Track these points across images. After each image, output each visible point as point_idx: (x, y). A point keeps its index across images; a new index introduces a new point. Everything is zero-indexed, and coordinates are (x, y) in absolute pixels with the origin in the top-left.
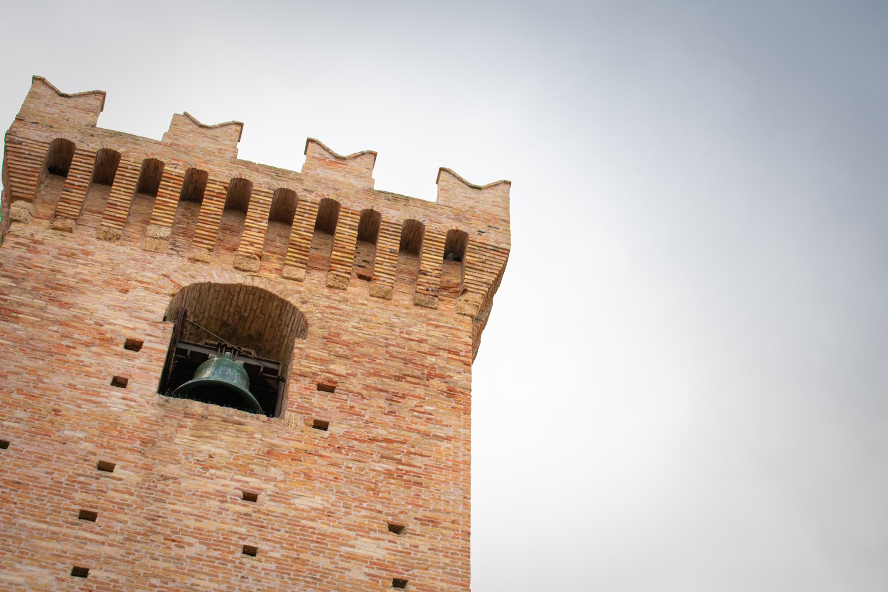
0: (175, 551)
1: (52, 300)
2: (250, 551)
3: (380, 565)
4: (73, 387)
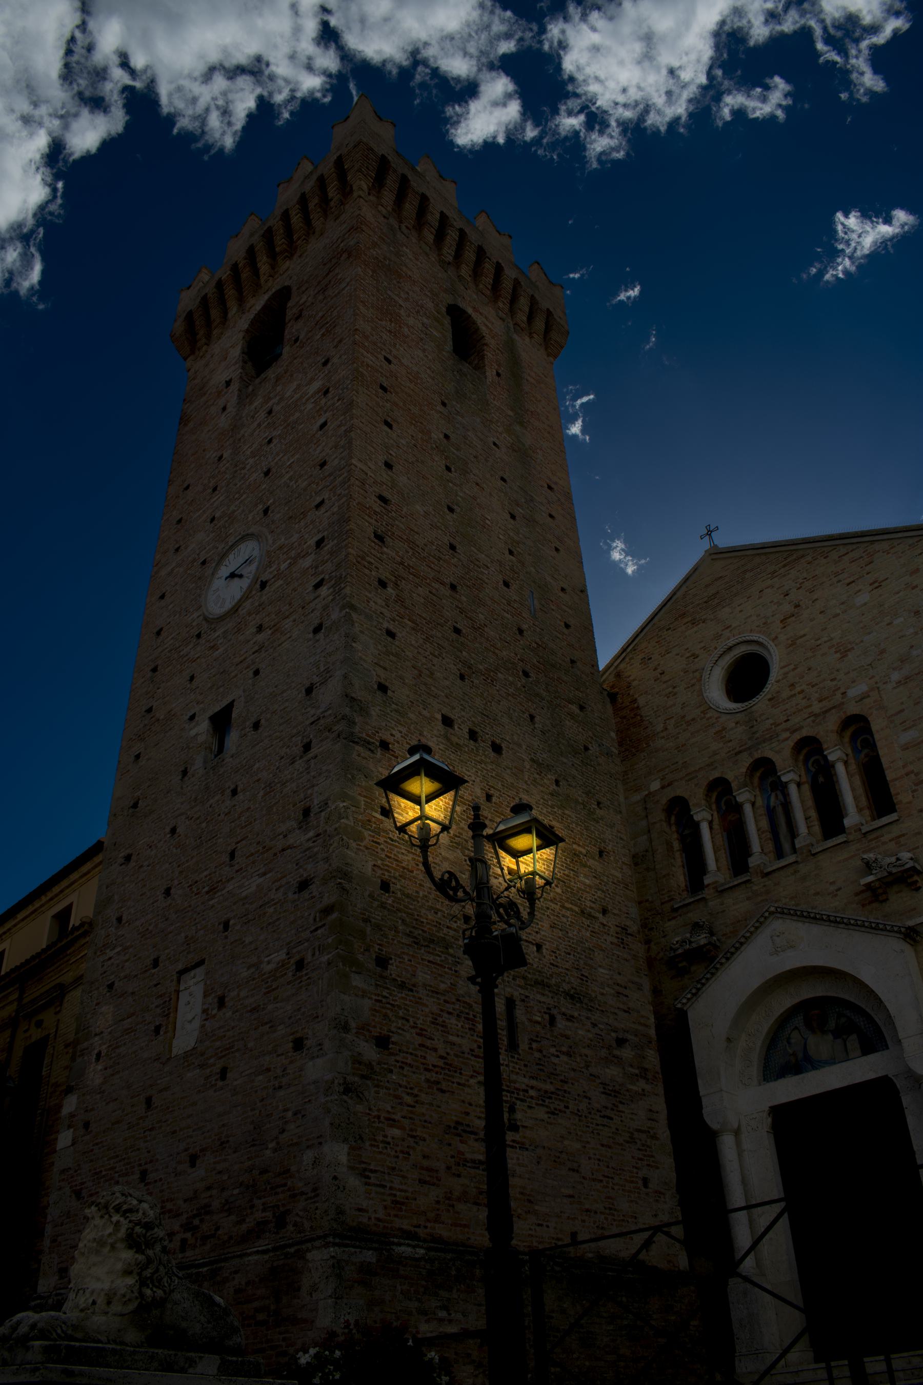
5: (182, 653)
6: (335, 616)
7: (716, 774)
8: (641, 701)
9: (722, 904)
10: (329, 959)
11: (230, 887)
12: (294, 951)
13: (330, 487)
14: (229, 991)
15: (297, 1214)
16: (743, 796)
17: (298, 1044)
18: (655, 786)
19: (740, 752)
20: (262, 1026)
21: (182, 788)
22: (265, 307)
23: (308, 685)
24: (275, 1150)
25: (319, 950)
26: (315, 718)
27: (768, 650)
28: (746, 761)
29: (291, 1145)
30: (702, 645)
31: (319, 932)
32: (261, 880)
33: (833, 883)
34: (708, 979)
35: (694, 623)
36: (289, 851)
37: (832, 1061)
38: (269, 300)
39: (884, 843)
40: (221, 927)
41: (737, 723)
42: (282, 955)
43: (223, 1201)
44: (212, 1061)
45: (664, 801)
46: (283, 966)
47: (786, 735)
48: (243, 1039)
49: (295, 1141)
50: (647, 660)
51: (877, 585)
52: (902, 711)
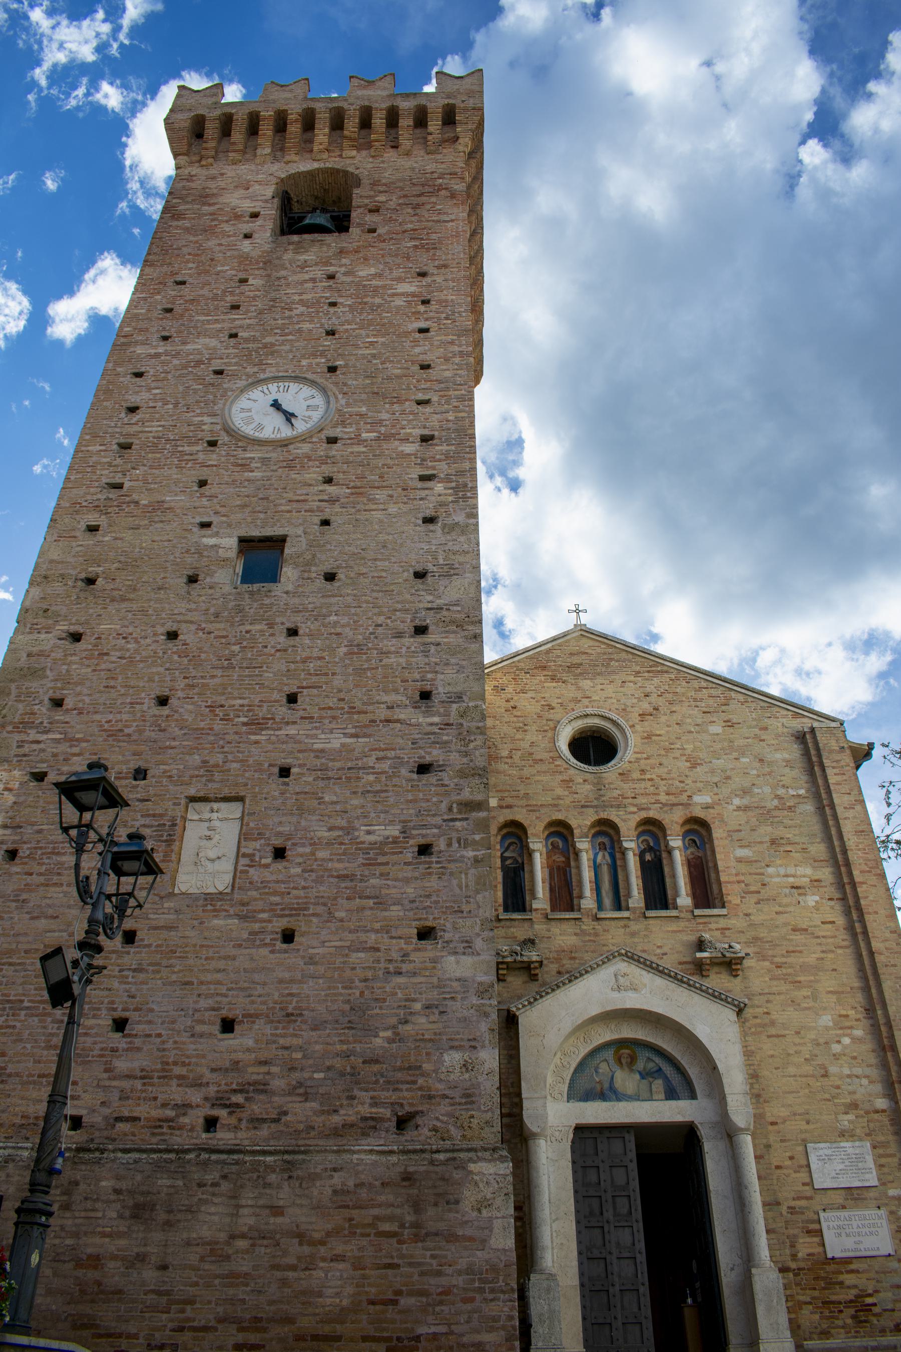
0: (287, 313)
1: (204, 204)
4: (220, 245)
5: (180, 449)
7: (560, 816)
9: (549, 931)
10: (475, 856)
11: (292, 730)
12: (414, 832)
14: (294, 844)
15: (437, 1119)
16: (583, 844)
19: (587, 806)
20: (360, 898)
21: (189, 593)
22: (310, 173)
23: (419, 568)
24: (390, 1041)
25: (459, 842)
26: (434, 605)
28: (591, 817)
29: (421, 1040)
31: (458, 824)
32: (348, 740)
34: (547, 993)
37: (636, 1098)
38: (318, 169)
39: (710, 930)
40: (276, 770)
41: (585, 781)
42: (394, 831)
43: (294, 1083)
44: (264, 916)
46: (394, 842)
47: (635, 809)
48: (325, 905)
49: (426, 1037)
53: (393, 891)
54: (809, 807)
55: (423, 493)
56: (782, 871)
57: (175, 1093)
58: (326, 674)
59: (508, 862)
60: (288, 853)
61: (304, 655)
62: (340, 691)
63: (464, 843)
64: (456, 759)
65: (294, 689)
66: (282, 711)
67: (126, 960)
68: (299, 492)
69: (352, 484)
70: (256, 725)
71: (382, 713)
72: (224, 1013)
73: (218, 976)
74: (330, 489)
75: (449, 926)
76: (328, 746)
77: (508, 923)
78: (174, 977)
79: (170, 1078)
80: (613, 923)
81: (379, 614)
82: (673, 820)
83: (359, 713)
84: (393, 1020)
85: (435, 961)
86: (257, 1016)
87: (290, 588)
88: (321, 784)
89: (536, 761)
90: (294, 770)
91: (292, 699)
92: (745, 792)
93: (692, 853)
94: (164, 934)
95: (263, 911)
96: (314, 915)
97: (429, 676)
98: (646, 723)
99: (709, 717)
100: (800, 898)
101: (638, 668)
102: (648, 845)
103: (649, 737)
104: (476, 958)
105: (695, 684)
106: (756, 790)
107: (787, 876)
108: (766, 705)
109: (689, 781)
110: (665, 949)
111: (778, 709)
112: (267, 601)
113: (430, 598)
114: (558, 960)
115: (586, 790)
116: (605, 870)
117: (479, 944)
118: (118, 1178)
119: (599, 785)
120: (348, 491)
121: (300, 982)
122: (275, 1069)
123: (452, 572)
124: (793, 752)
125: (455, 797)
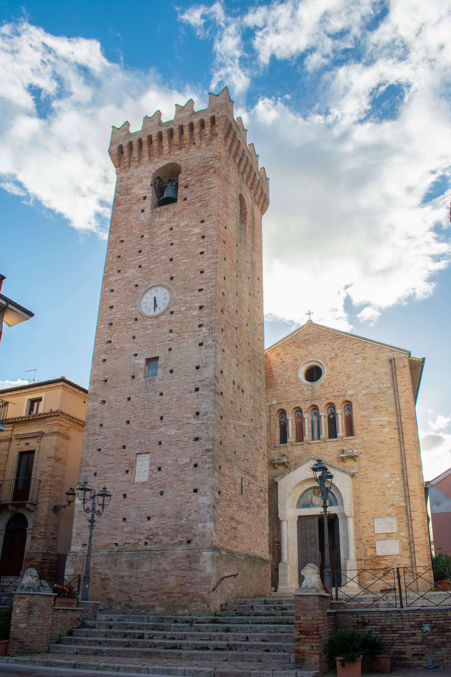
2: (172, 244)
3: (199, 234)
6: (210, 342)
7: (298, 405)
8: (274, 369)
9: (292, 449)
11: (161, 429)
12: (193, 460)
13: (206, 285)
16: (305, 416)
17: (195, 491)
18: (275, 402)
23: (197, 365)
24: (186, 521)
27: (323, 367)
28: (309, 404)
30: (300, 356)
31: (204, 457)
32: (177, 431)
33: (330, 452)
35: (298, 347)
36: (190, 425)
39: (349, 444)
40: (158, 443)
42: (188, 460)
44: (156, 488)
45: (277, 409)
50: (278, 355)
51: (364, 358)
52: (363, 404)
53: (187, 479)
54: (391, 392)
55: (199, 333)
56: (377, 419)
57: (137, 536)
58: (170, 409)
59: (282, 423)
60: (161, 469)
61: (165, 402)
62: (174, 414)
63: (206, 463)
64: (205, 435)
65: (162, 415)
66: (159, 423)
67: (125, 502)
68: (162, 338)
69: (178, 332)
70: (153, 428)
71: (185, 421)
72: (148, 515)
73: (146, 505)
74: (171, 335)
75: (201, 488)
76: (171, 434)
77: (279, 448)
78: (136, 506)
79: (136, 533)
80: (314, 445)
81: (185, 385)
82: (338, 403)
83: (179, 421)
84: (187, 515)
85: (197, 498)
86: (155, 516)
87: (160, 378)
88: (169, 446)
89: (290, 384)
90: (162, 443)
91: (162, 418)
92: (367, 387)
93: (348, 413)
94: (133, 494)
95: (155, 486)
96: (168, 487)
97: (199, 406)
98: (332, 362)
99: (357, 356)
100: (383, 430)
101: (331, 338)
102: (332, 412)
103: (332, 368)
104: (207, 497)
105: (353, 342)
106: (371, 386)
107: (379, 421)
108: (380, 347)
109: (346, 385)
110: (332, 453)
111: (384, 349)
112: (154, 383)
113: (200, 377)
114: (295, 460)
115: (308, 393)
116: (316, 423)
117: (208, 493)
118: (126, 558)
119: (313, 391)
120: (177, 335)
121: (165, 506)
122: (160, 529)
123: (207, 365)
124: (387, 368)
125: (204, 448)
